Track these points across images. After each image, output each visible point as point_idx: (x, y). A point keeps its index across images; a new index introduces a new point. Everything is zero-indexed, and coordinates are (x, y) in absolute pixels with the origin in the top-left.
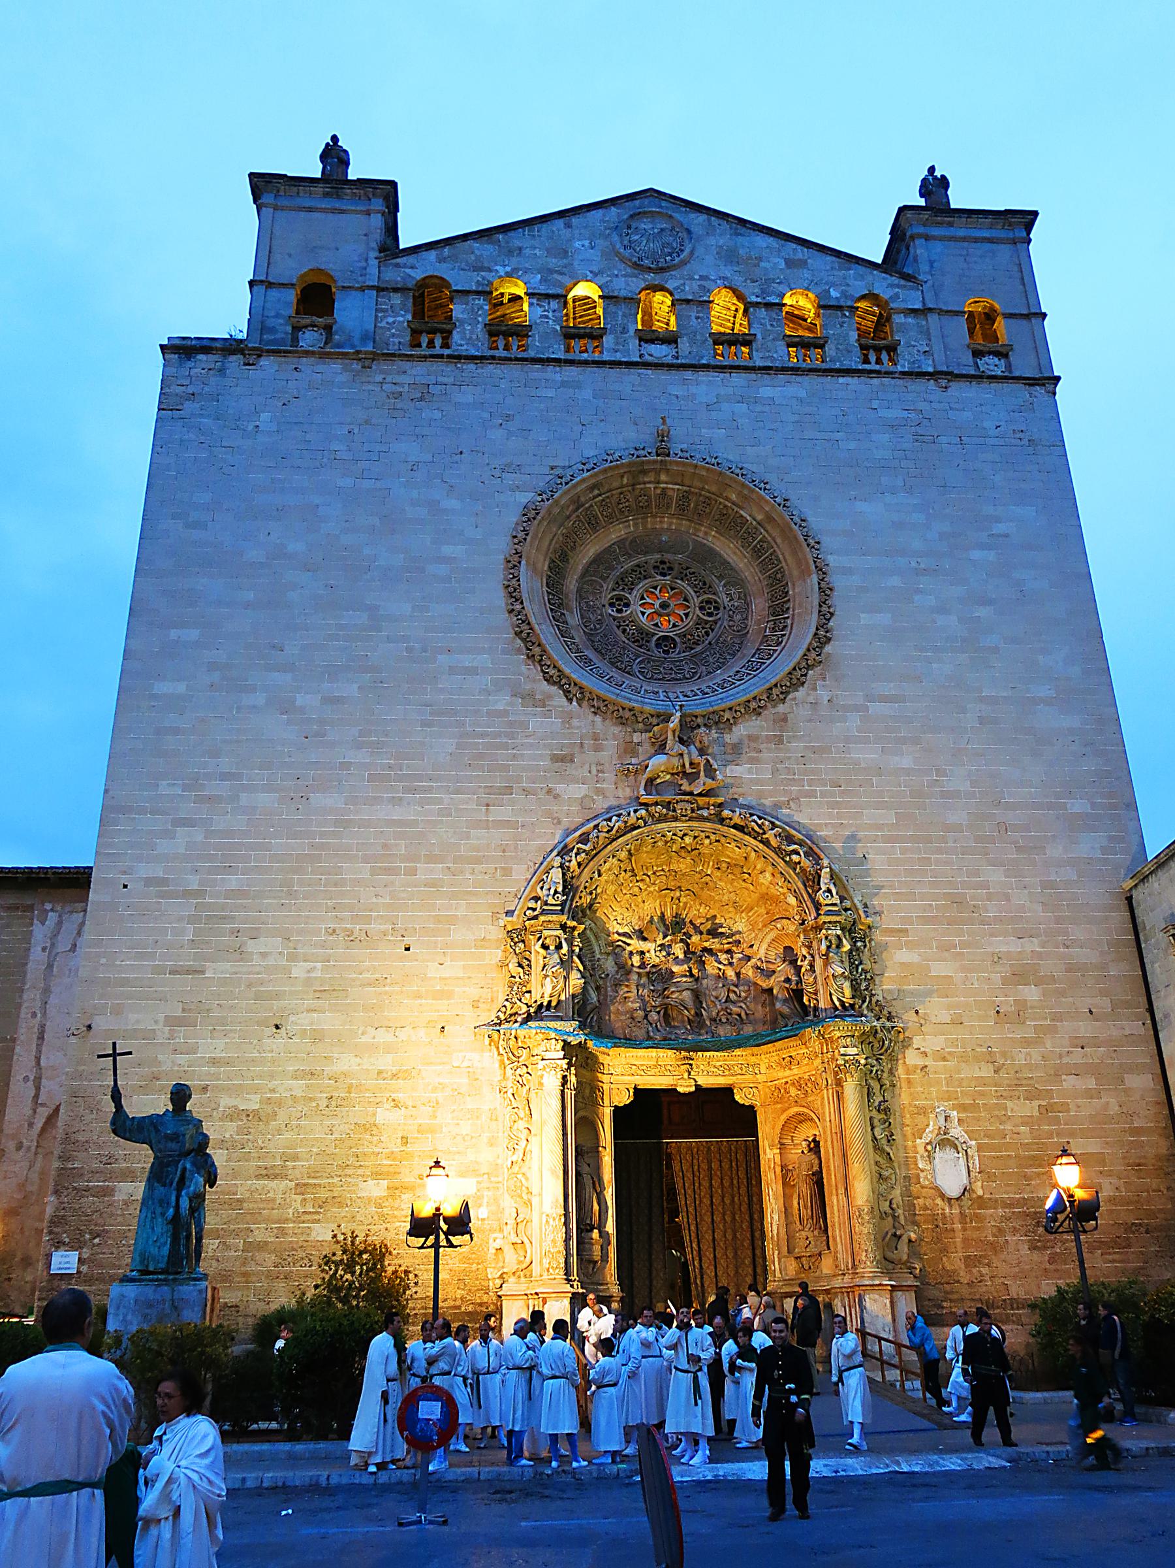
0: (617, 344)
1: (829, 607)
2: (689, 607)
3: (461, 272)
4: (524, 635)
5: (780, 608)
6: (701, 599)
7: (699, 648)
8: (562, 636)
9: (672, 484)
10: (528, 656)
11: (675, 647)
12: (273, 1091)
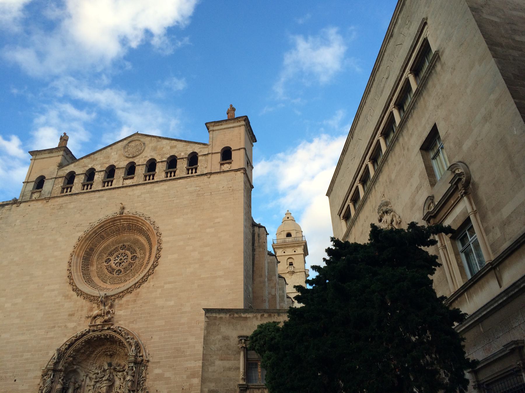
0: (117, 182)
1: (159, 255)
3: (79, 169)
4: (69, 277)
6: (132, 256)
7: (128, 271)
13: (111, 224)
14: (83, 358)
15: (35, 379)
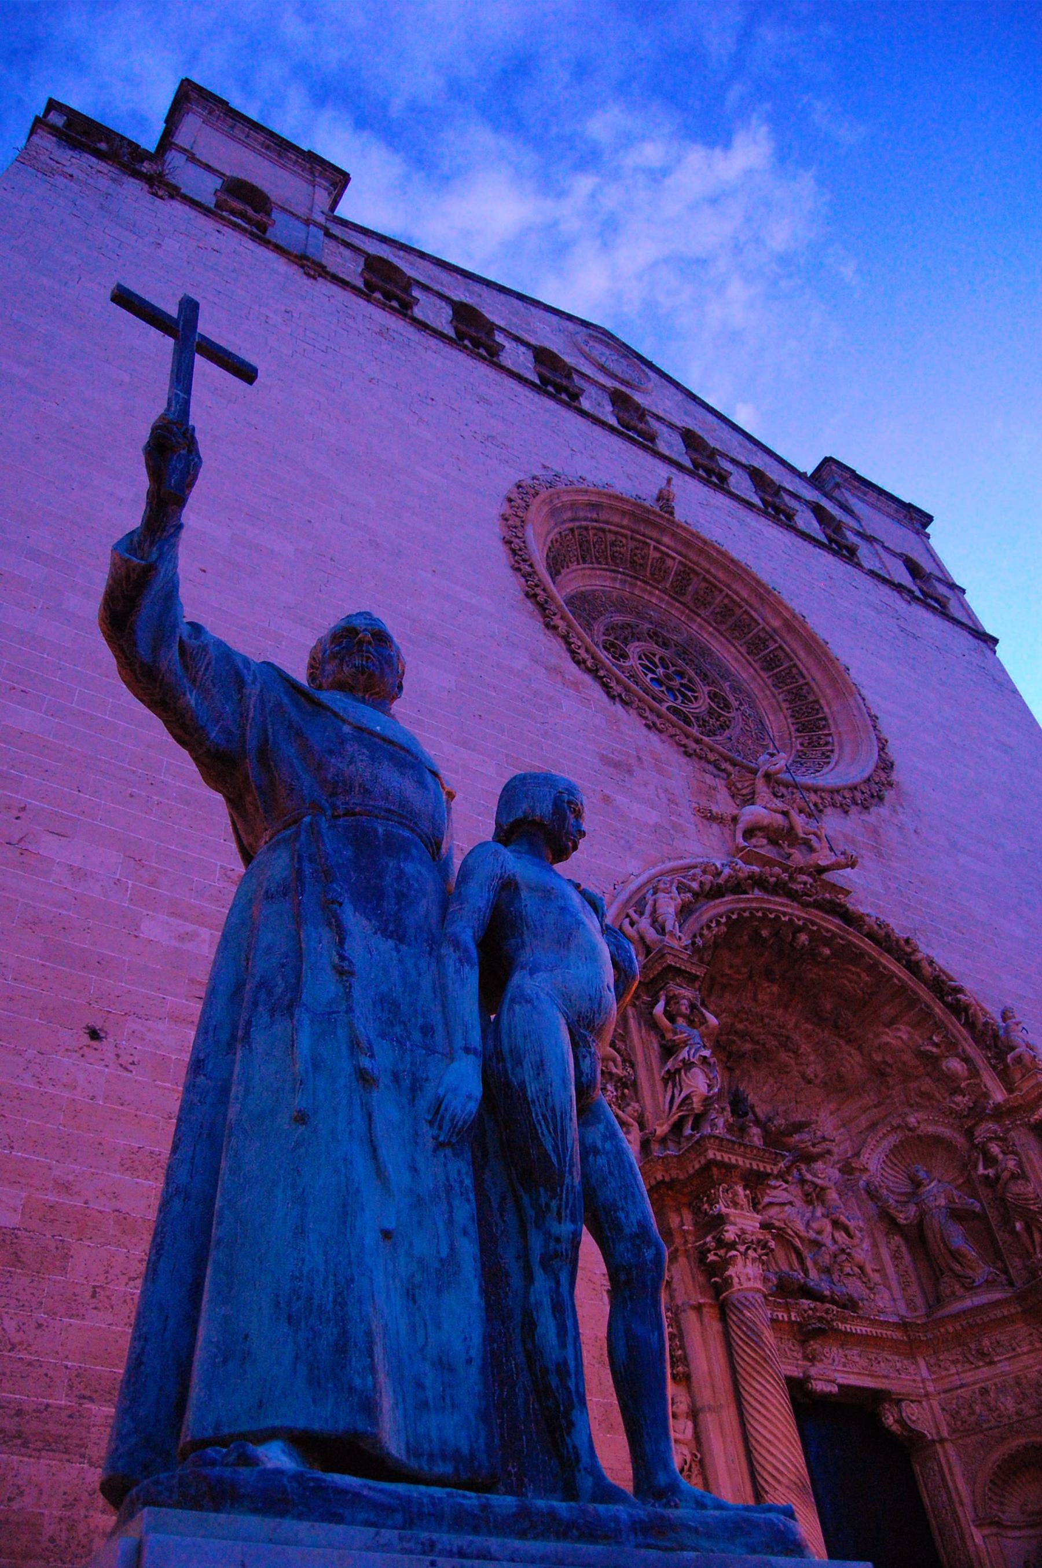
9: (672, 550)
12: (65, 1187)
13: (625, 522)
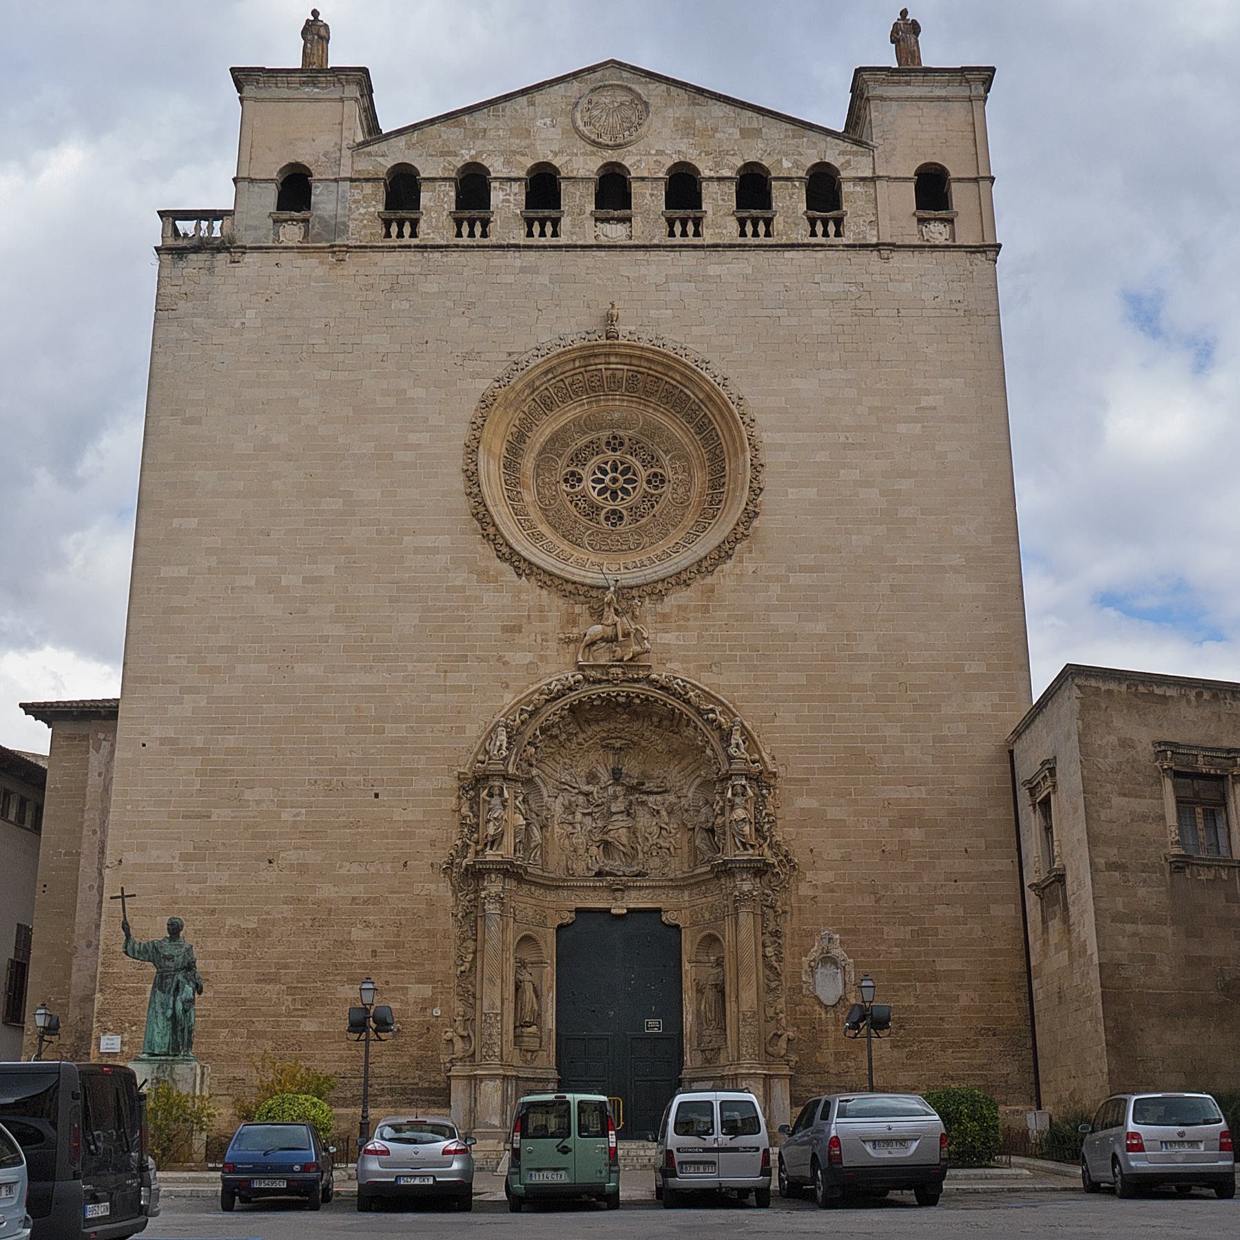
0: (574, 226)
2: (636, 481)
4: (480, 516)
5: (717, 482)
6: (648, 472)
7: (643, 521)
8: (516, 515)
10: (483, 535)
11: (621, 518)
12: (267, 913)
13: (577, 364)
14: (549, 750)
15: (439, 795)
